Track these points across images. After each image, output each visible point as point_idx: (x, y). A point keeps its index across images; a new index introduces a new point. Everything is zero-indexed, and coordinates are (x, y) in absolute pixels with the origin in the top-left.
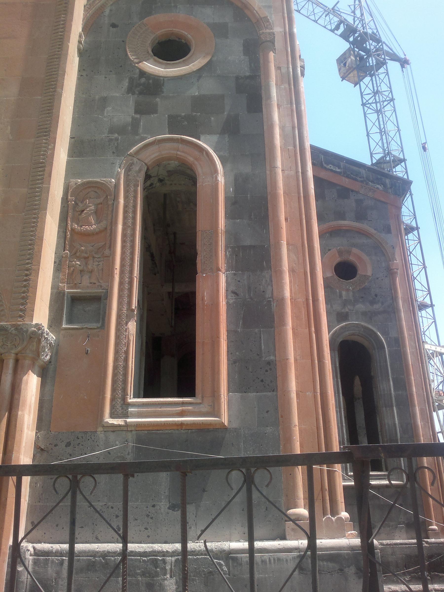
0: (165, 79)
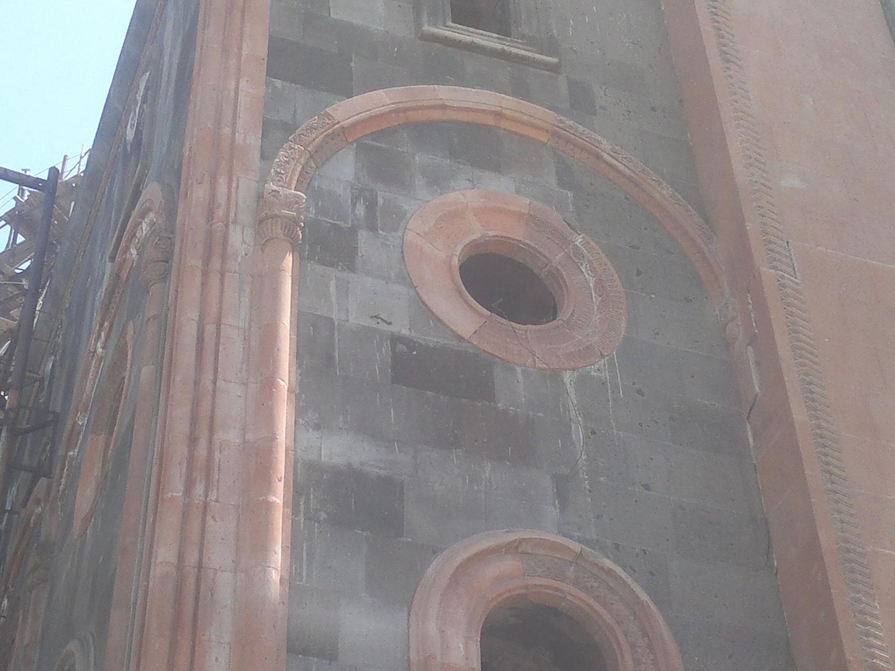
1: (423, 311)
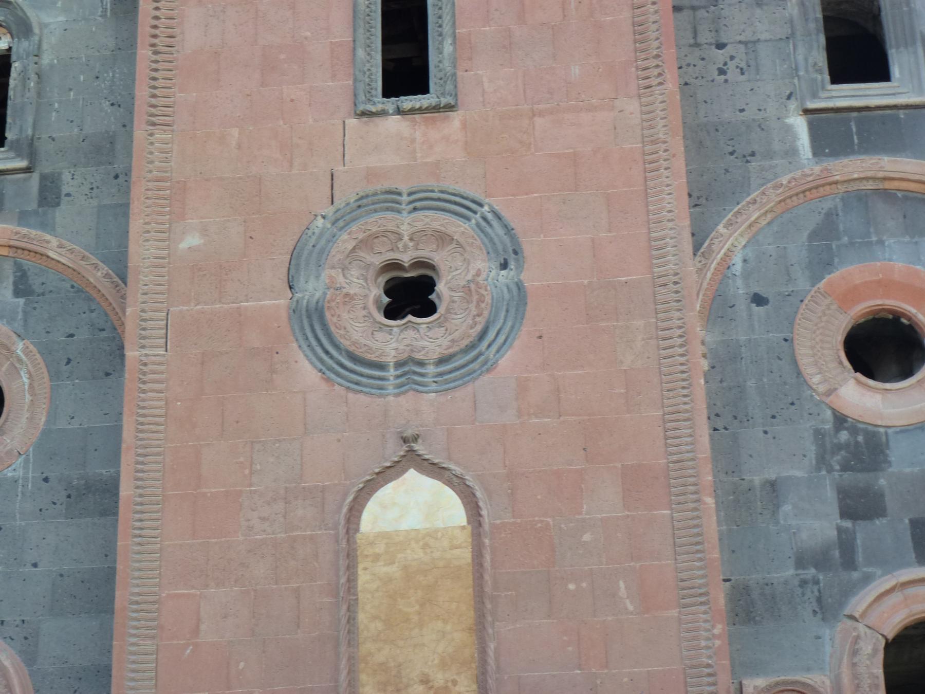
0: (890, 431)
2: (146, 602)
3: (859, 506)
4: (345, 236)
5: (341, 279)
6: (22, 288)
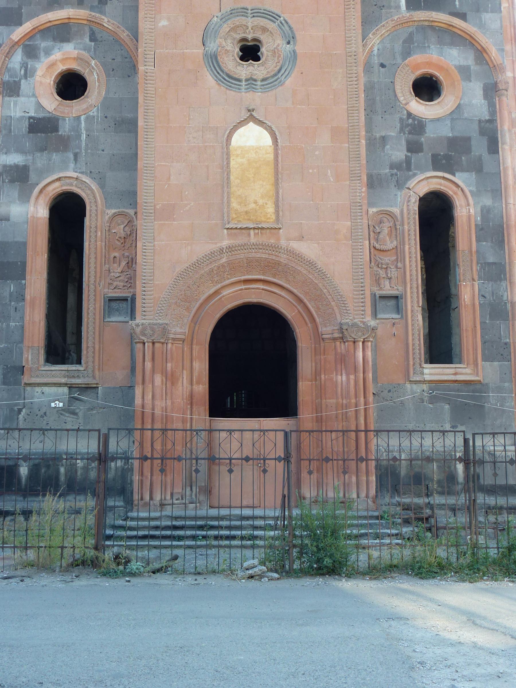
1: (39, 106)
2: (150, 167)
3: (414, 147)
4: (225, 26)
5: (224, 43)
6: (93, 38)
